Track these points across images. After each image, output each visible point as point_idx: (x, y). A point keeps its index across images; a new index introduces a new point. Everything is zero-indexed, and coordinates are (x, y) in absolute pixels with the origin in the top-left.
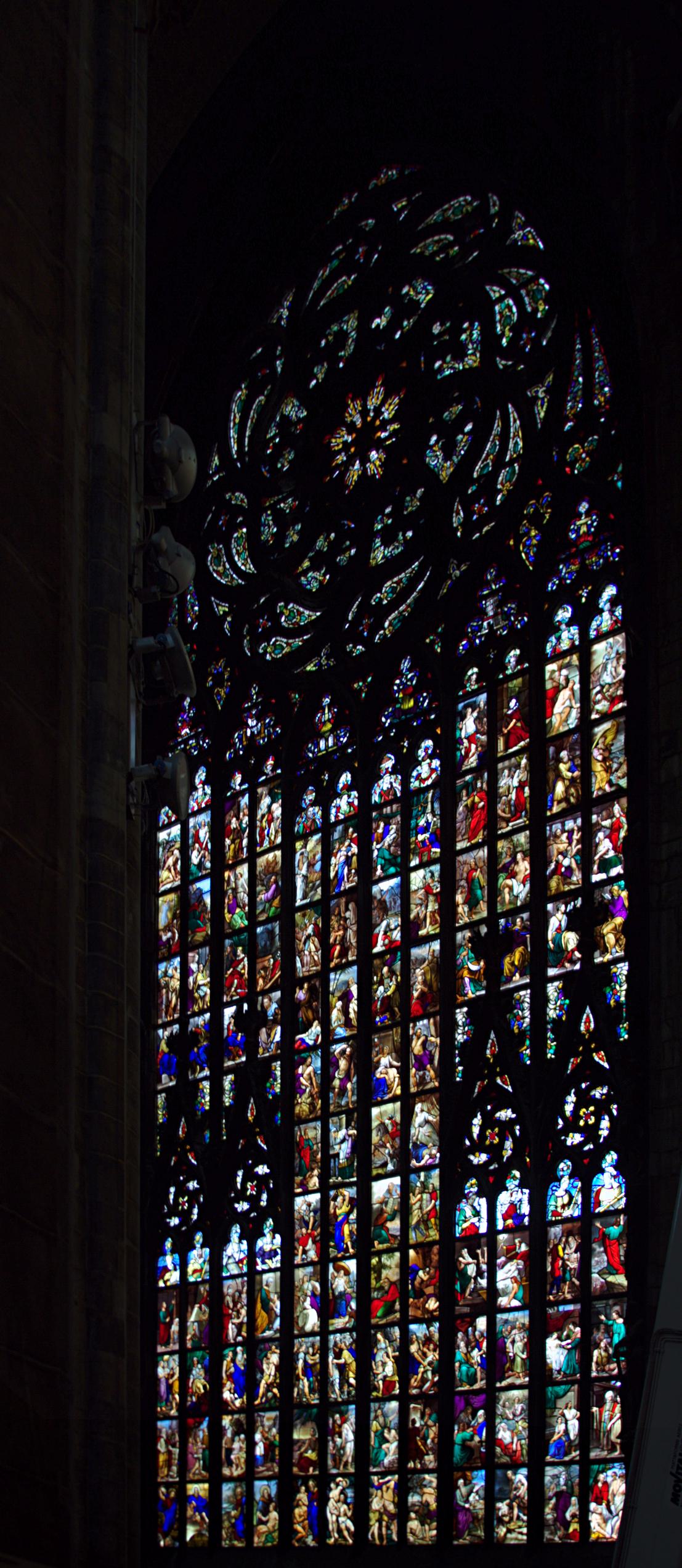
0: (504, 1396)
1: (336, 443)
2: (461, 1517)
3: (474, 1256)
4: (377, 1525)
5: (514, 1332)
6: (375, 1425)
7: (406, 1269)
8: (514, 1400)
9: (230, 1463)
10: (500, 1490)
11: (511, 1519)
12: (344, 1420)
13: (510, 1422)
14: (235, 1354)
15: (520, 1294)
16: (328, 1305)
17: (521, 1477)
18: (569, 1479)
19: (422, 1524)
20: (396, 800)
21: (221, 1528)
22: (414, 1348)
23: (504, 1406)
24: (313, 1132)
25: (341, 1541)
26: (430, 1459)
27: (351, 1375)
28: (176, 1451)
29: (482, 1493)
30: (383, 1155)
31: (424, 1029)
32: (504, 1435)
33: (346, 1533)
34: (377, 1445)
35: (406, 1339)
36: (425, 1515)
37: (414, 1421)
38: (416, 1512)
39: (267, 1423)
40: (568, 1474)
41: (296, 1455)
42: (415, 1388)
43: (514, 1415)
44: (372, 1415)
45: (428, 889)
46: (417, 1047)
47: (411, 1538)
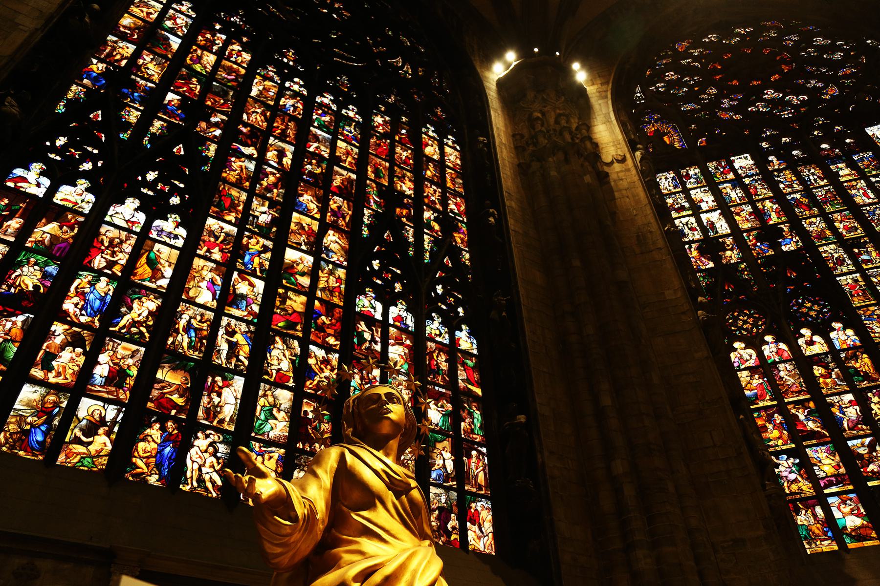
6: (262, 401)
25: (199, 490)
34: (262, 417)
35: (305, 354)
39: (121, 351)
41: (155, 393)
44: (261, 393)
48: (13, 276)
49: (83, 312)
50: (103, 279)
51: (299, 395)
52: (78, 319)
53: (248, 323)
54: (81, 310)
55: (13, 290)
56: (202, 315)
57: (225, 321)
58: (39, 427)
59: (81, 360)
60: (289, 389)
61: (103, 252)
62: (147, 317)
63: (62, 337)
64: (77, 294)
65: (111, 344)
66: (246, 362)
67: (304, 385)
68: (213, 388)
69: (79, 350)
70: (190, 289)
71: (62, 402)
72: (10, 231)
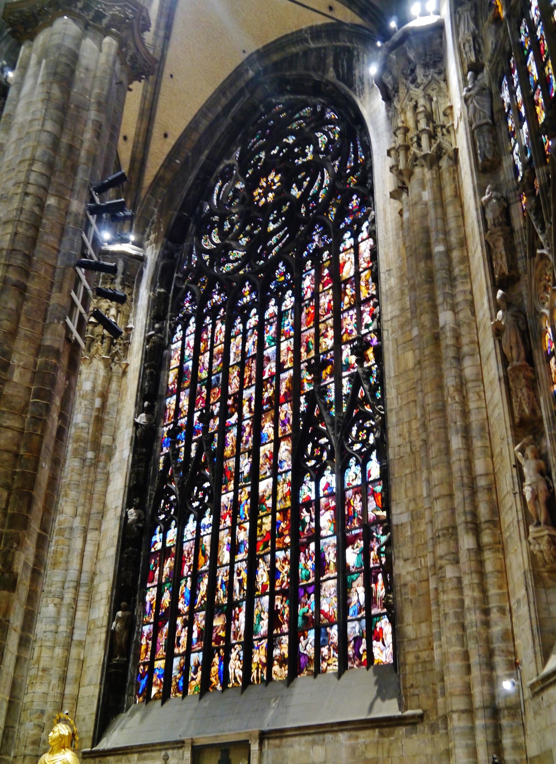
1: (255, 193)
2: (302, 660)
3: (308, 511)
6: (256, 611)
7: (275, 523)
8: (330, 587)
9: (179, 645)
10: (324, 640)
12: (240, 611)
14: (186, 581)
15: (332, 528)
16: (234, 548)
17: (334, 631)
18: (361, 628)
19: (281, 667)
20: (275, 316)
21: (171, 686)
22: (278, 565)
24: (231, 463)
25: (236, 684)
26: (285, 628)
27: (245, 584)
28: (150, 642)
29: (313, 643)
30: (265, 469)
31: (286, 409)
32: (325, 607)
33: (238, 679)
36: (282, 662)
38: (277, 660)
40: (360, 626)
41: (214, 635)
45: (288, 349)
46: (282, 416)
47: (274, 677)
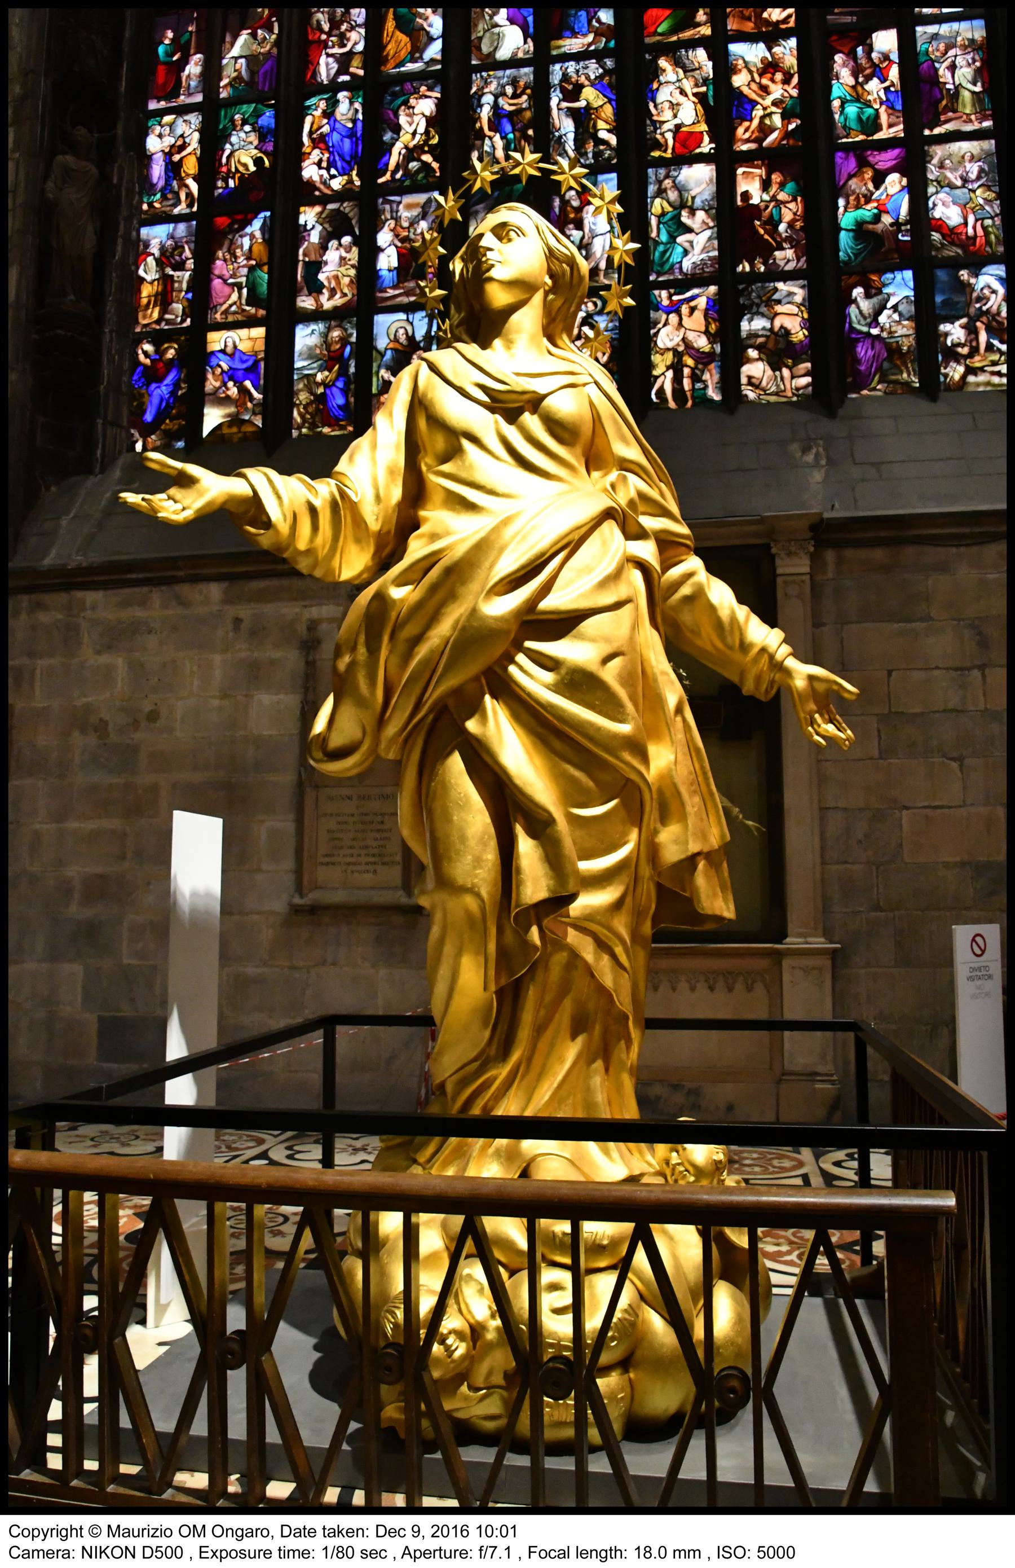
0: (938, 152)
2: (862, 351)
4: (670, 374)
5: (952, 52)
6: (657, 206)
9: (315, 288)
11: (974, 351)
13: (958, 192)
14: (333, 103)
19: (775, 367)
22: (739, 80)
23: (941, 166)
26: (786, 257)
34: (664, 237)
35: (724, 67)
36: (779, 351)
37: (746, 195)
38: (759, 348)
39: (405, 214)
42: (747, 141)
43: (965, 180)
44: (652, 189)
48: (224, 160)
49: (333, 171)
50: (342, 95)
51: (726, 163)
52: (329, 187)
53: (598, 56)
54: (328, 169)
55: (231, 183)
56: (514, 82)
57: (556, 71)
58: (334, 385)
59: (354, 255)
60: (703, 158)
61: (326, 47)
62: (427, 132)
63: (319, 228)
64: (315, 143)
65: (387, 207)
66: (613, 140)
67: (732, 138)
68: (566, 215)
69: (347, 240)
70: (480, 39)
71: (351, 335)
72: (193, 84)
